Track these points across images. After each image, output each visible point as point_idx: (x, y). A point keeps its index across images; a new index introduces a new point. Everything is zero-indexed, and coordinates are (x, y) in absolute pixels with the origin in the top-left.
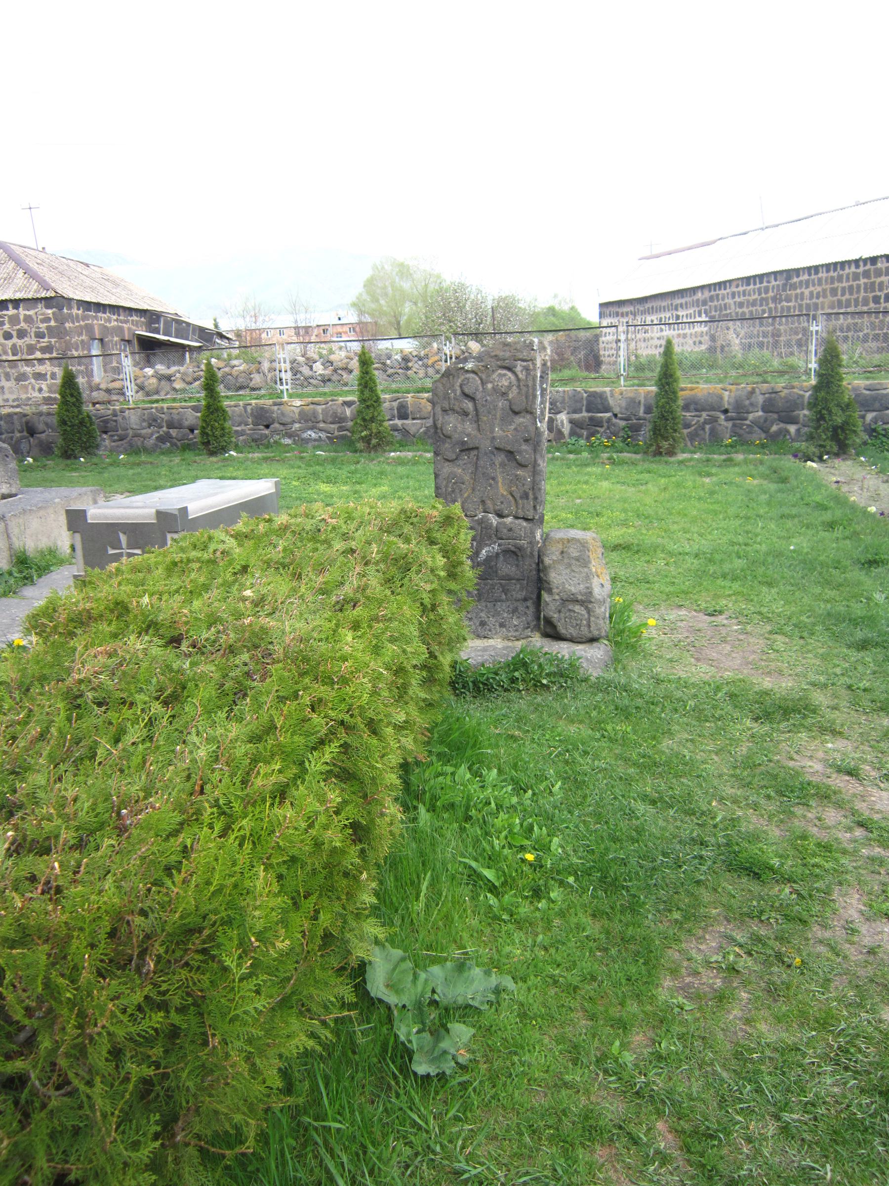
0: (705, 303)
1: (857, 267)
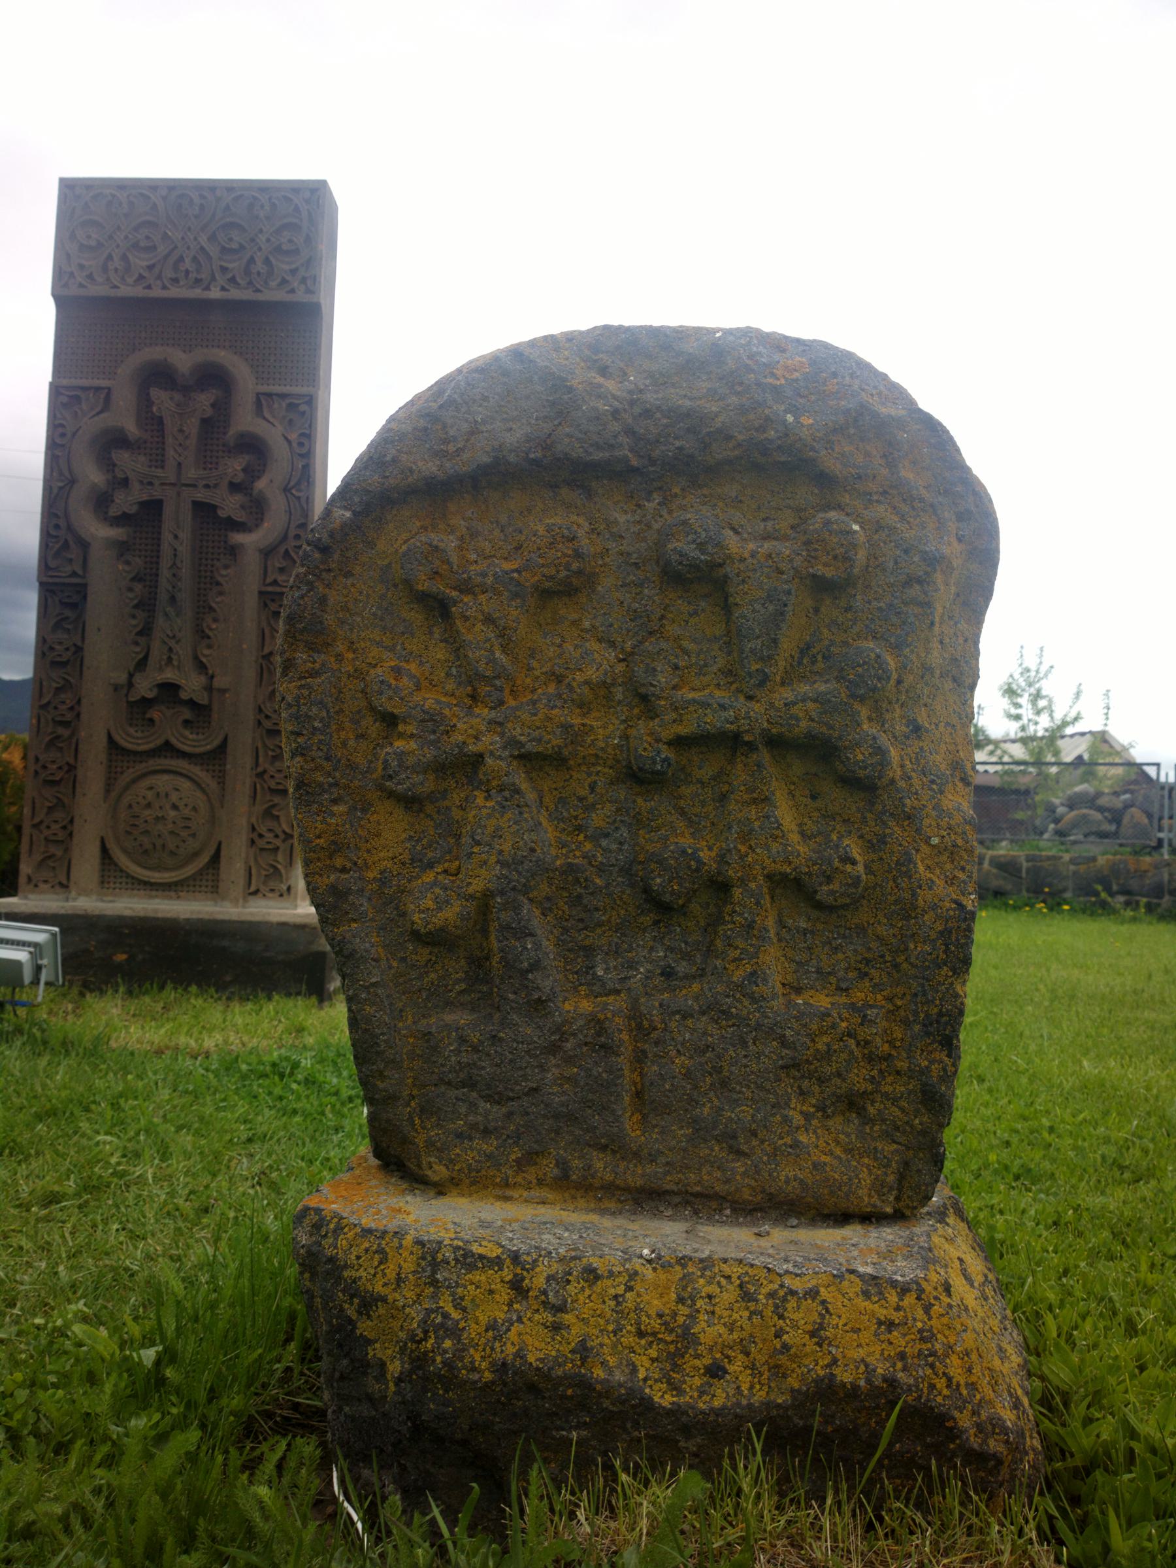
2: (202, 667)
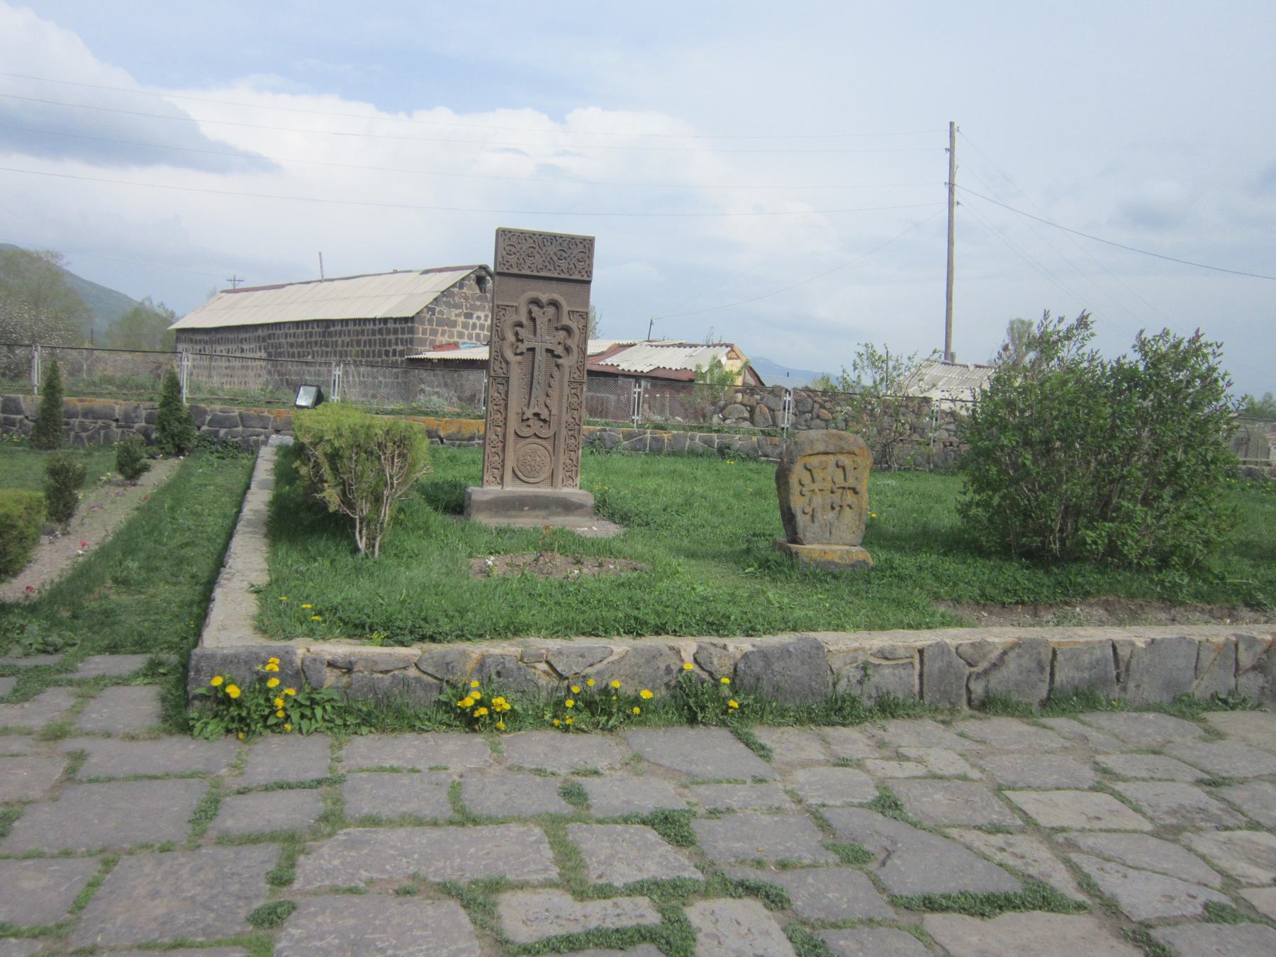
0: (264, 339)
1: (375, 324)
2: (547, 406)
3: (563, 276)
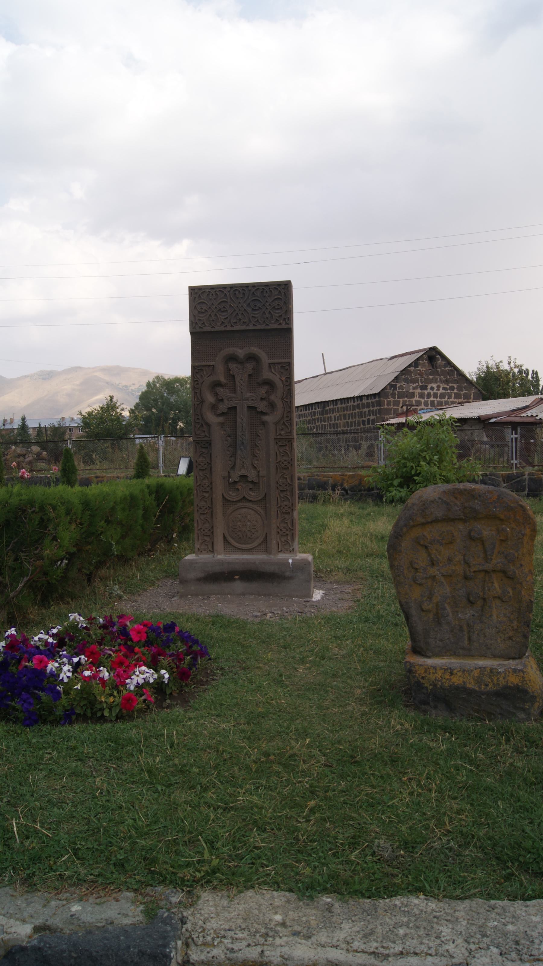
1: (354, 402)
2: (255, 468)
3: (259, 327)
